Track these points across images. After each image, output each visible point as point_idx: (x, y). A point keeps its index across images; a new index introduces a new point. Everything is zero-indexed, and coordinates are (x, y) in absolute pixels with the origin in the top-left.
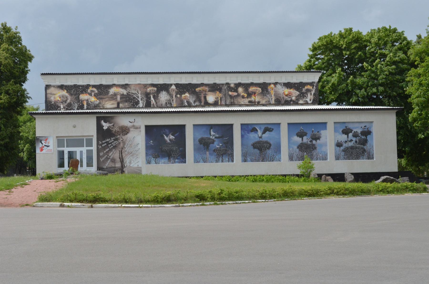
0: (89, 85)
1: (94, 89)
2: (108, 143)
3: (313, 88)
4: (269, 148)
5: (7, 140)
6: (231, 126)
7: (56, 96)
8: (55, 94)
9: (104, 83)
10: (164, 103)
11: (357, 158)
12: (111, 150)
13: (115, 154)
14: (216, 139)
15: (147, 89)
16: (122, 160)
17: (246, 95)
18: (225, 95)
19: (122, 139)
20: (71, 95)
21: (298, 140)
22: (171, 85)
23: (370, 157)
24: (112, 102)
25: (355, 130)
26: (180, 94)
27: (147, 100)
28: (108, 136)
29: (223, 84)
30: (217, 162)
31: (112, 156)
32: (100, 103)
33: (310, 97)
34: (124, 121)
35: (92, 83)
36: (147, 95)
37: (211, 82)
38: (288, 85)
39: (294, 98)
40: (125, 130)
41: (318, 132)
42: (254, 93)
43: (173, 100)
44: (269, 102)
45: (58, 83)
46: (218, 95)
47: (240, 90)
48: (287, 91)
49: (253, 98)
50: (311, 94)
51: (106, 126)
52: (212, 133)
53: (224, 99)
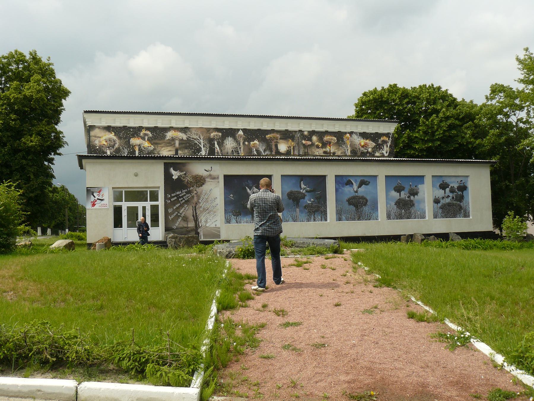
0: (142, 127)
1: (148, 132)
2: (178, 196)
3: (389, 139)
4: (365, 204)
5: (39, 192)
6: (324, 177)
7: (101, 139)
8: (100, 137)
9: (160, 125)
10: (230, 151)
11: (455, 216)
12: (182, 206)
13: (188, 211)
14: (306, 194)
15: (210, 134)
16: (197, 218)
17: (320, 145)
18: (298, 144)
19: (195, 192)
20: (120, 138)
21: (395, 195)
22: (238, 130)
23: (466, 215)
24: (169, 148)
25: (452, 185)
26: (248, 142)
27: (210, 147)
28: (180, 188)
29: (296, 132)
30: (309, 221)
31: (184, 213)
32: (154, 149)
33: (386, 150)
34: (199, 169)
35: (145, 125)
36: (211, 141)
37: (283, 128)
38: (364, 135)
39: (370, 150)
40: (200, 181)
41: (416, 186)
42: (329, 143)
43: (240, 148)
44: (345, 153)
45: (104, 124)
46: (291, 143)
47: (314, 138)
48: (363, 142)
49: (328, 149)
50: (387, 146)
51: (175, 174)
52: (303, 186)
53: (297, 148)
